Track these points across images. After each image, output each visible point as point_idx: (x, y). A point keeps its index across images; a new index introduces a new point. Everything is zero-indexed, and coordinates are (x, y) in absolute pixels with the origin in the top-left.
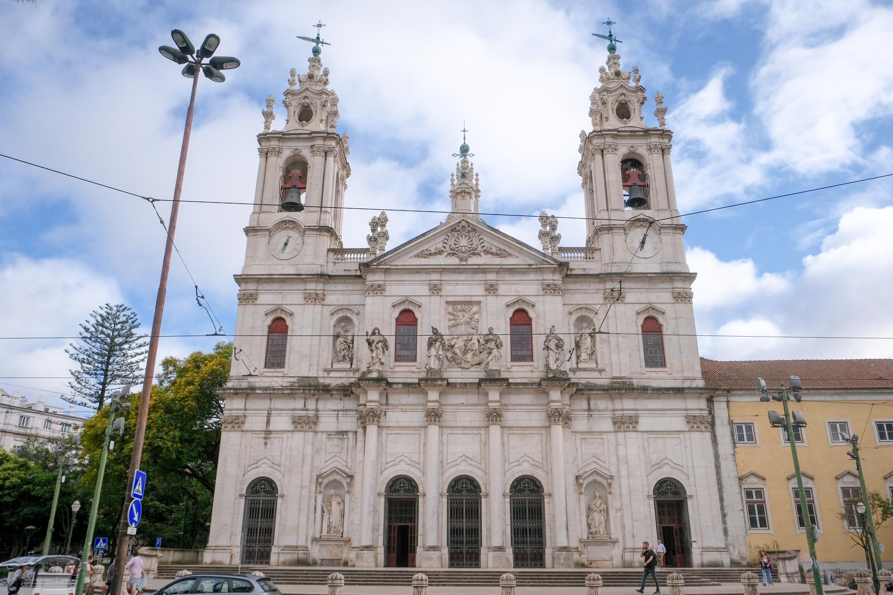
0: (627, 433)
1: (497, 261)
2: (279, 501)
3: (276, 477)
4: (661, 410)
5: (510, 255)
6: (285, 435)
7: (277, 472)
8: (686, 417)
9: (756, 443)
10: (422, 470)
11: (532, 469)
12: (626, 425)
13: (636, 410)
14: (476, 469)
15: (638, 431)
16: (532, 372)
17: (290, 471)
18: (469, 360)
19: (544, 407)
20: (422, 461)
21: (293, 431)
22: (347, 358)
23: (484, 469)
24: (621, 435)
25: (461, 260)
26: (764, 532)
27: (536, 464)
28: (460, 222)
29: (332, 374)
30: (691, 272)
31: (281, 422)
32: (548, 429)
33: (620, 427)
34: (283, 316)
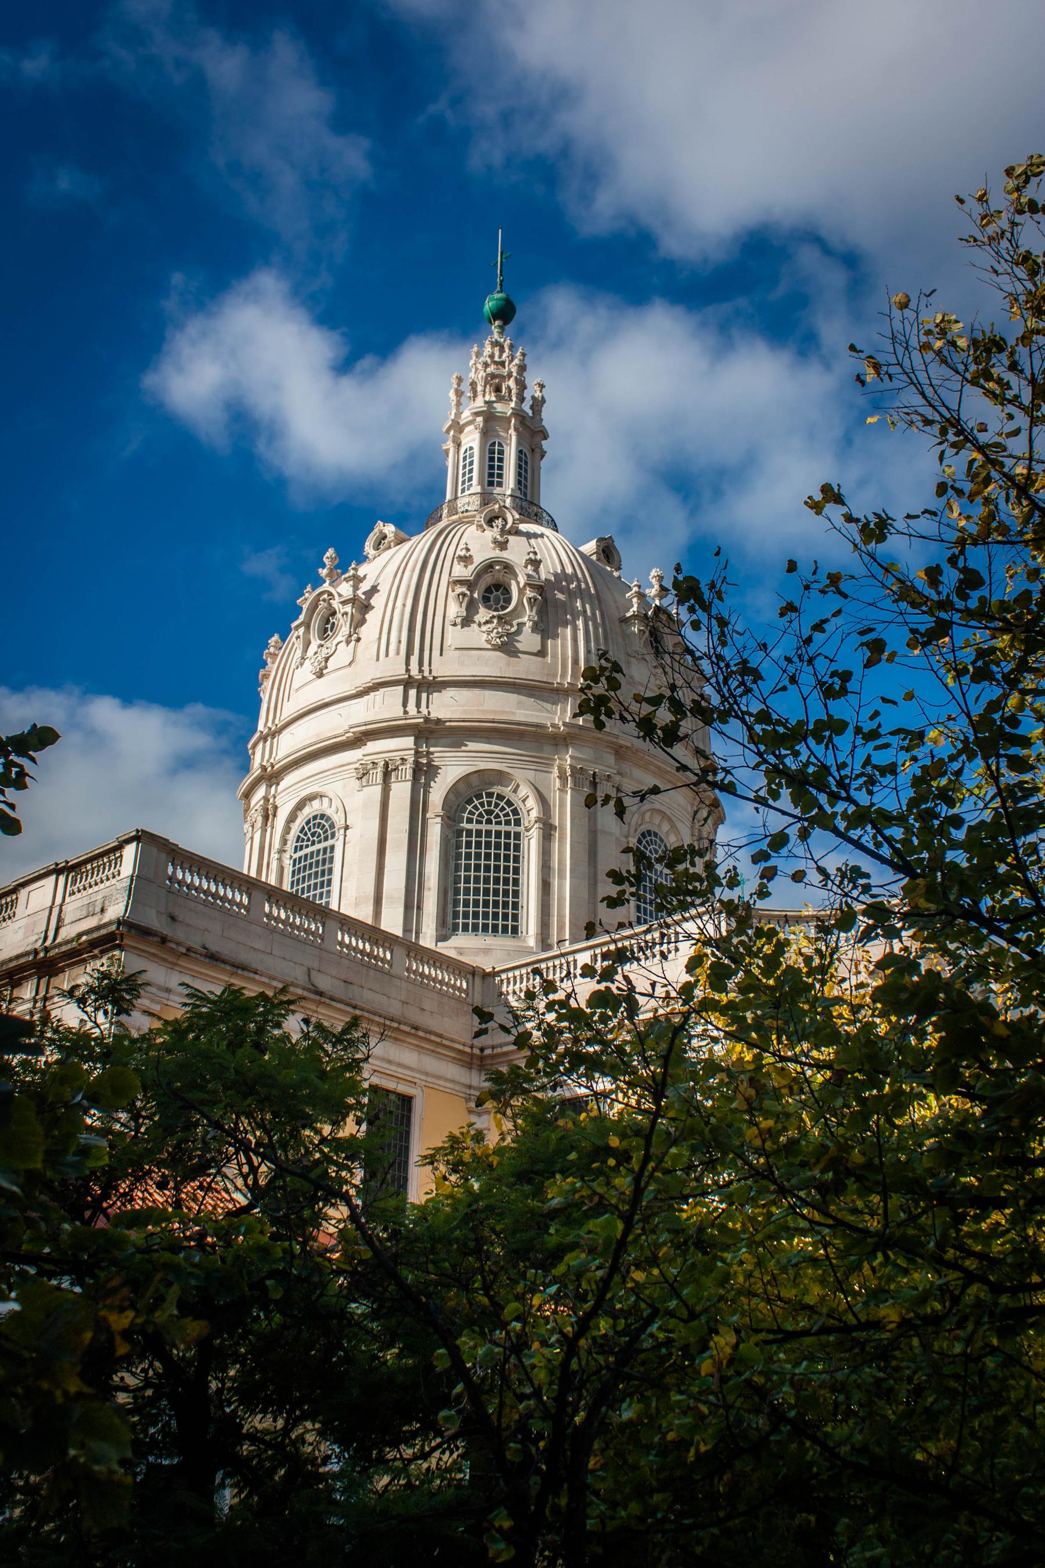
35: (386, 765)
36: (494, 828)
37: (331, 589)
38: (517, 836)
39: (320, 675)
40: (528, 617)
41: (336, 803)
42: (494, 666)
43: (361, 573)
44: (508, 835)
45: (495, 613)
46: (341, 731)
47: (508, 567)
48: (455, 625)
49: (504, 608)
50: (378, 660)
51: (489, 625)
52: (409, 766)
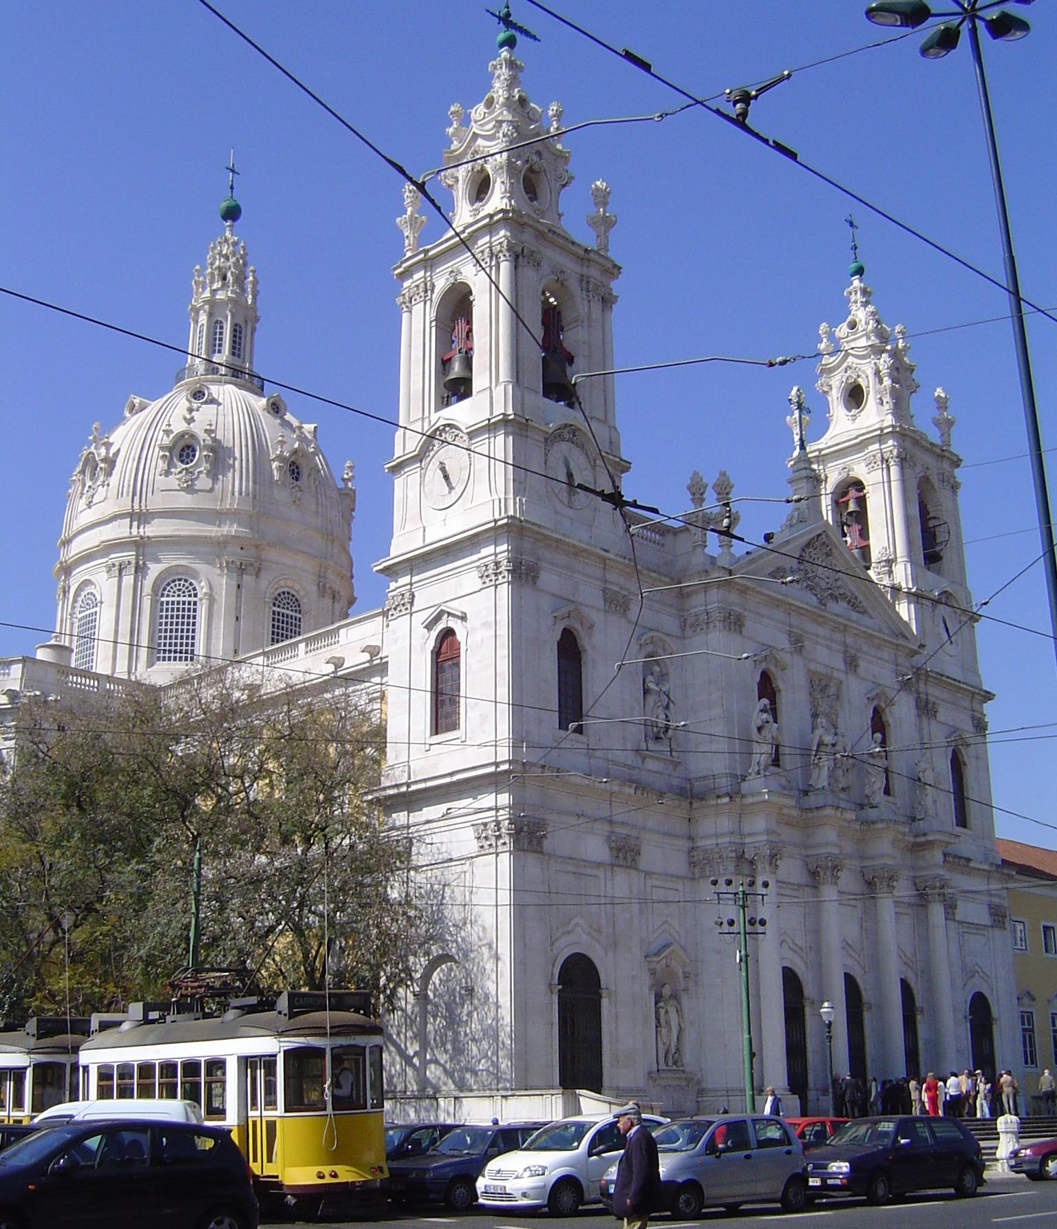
1: (855, 616)
2: (605, 1002)
3: (597, 956)
5: (864, 612)
6: (600, 873)
7: (598, 947)
8: (990, 906)
9: (1026, 949)
14: (856, 964)
17: (615, 944)
21: (613, 865)
22: (663, 736)
25: (820, 602)
26: (1033, 1070)
27: (908, 961)
28: (819, 535)
29: (651, 765)
30: (984, 688)
31: (596, 848)
32: (915, 908)
34: (578, 626)
35: (120, 565)
36: (182, 599)
37: (94, 451)
38: (195, 603)
39: (90, 507)
40: (204, 467)
41: (98, 588)
42: (185, 501)
43: (111, 440)
44: (189, 603)
45: (184, 466)
46: (97, 544)
47: (193, 436)
48: (161, 475)
49: (192, 461)
50: (118, 498)
51: (181, 475)
52: (133, 565)
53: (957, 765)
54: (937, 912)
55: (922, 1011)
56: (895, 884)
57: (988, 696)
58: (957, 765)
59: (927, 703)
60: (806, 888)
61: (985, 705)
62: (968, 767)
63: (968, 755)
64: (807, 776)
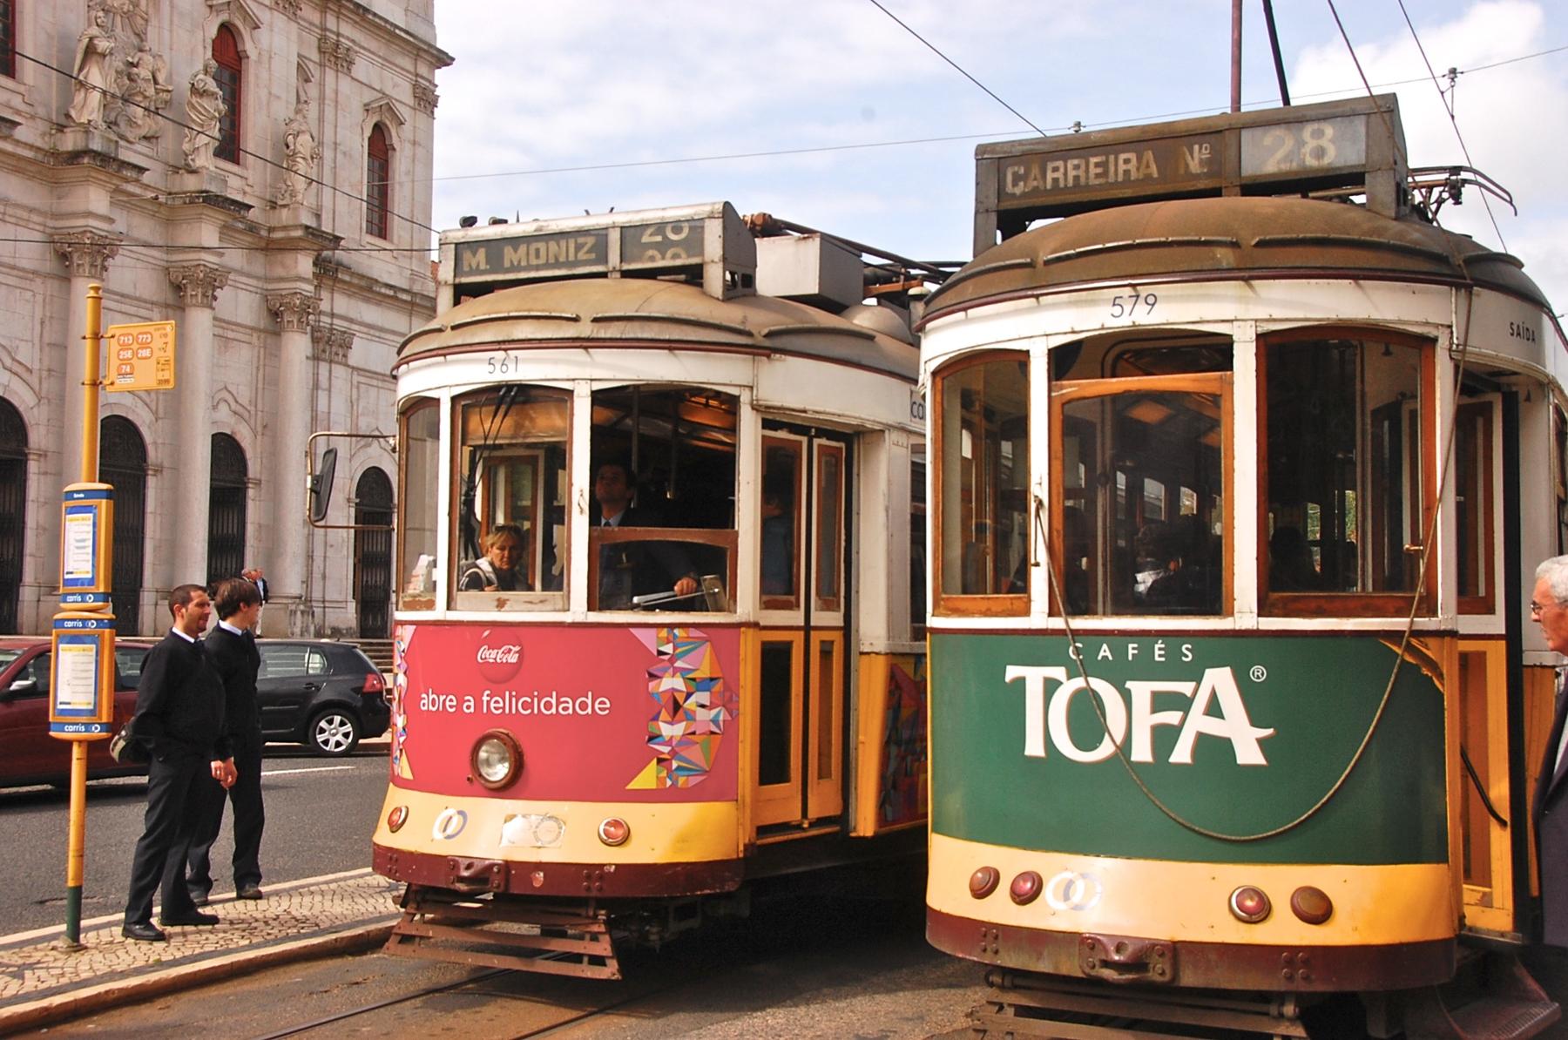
0: (333, 366)
4: (382, 329)
10: (37, 388)
11: (233, 420)
12: (334, 349)
13: (351, 321)
14: (140, 403)
15: (348, 366)
16: (245, 193)
18: (140, 122)
19: (260, 284)
20: (36, 366)
23: (154, 408)
24: (324, 368)
30: (439, 46)
32: (263, 336)
33: (324, 351)
53: (380, 148)
54: (297, 345)
55: (258, 483)
56: (218, 292)
57: (444, 60)
58: (380, 148)
59: (337, 45)
60: (49, 282)
61: (437, 71)
62: (398, 154)
63: (399, 138)
64: (67, 100)
